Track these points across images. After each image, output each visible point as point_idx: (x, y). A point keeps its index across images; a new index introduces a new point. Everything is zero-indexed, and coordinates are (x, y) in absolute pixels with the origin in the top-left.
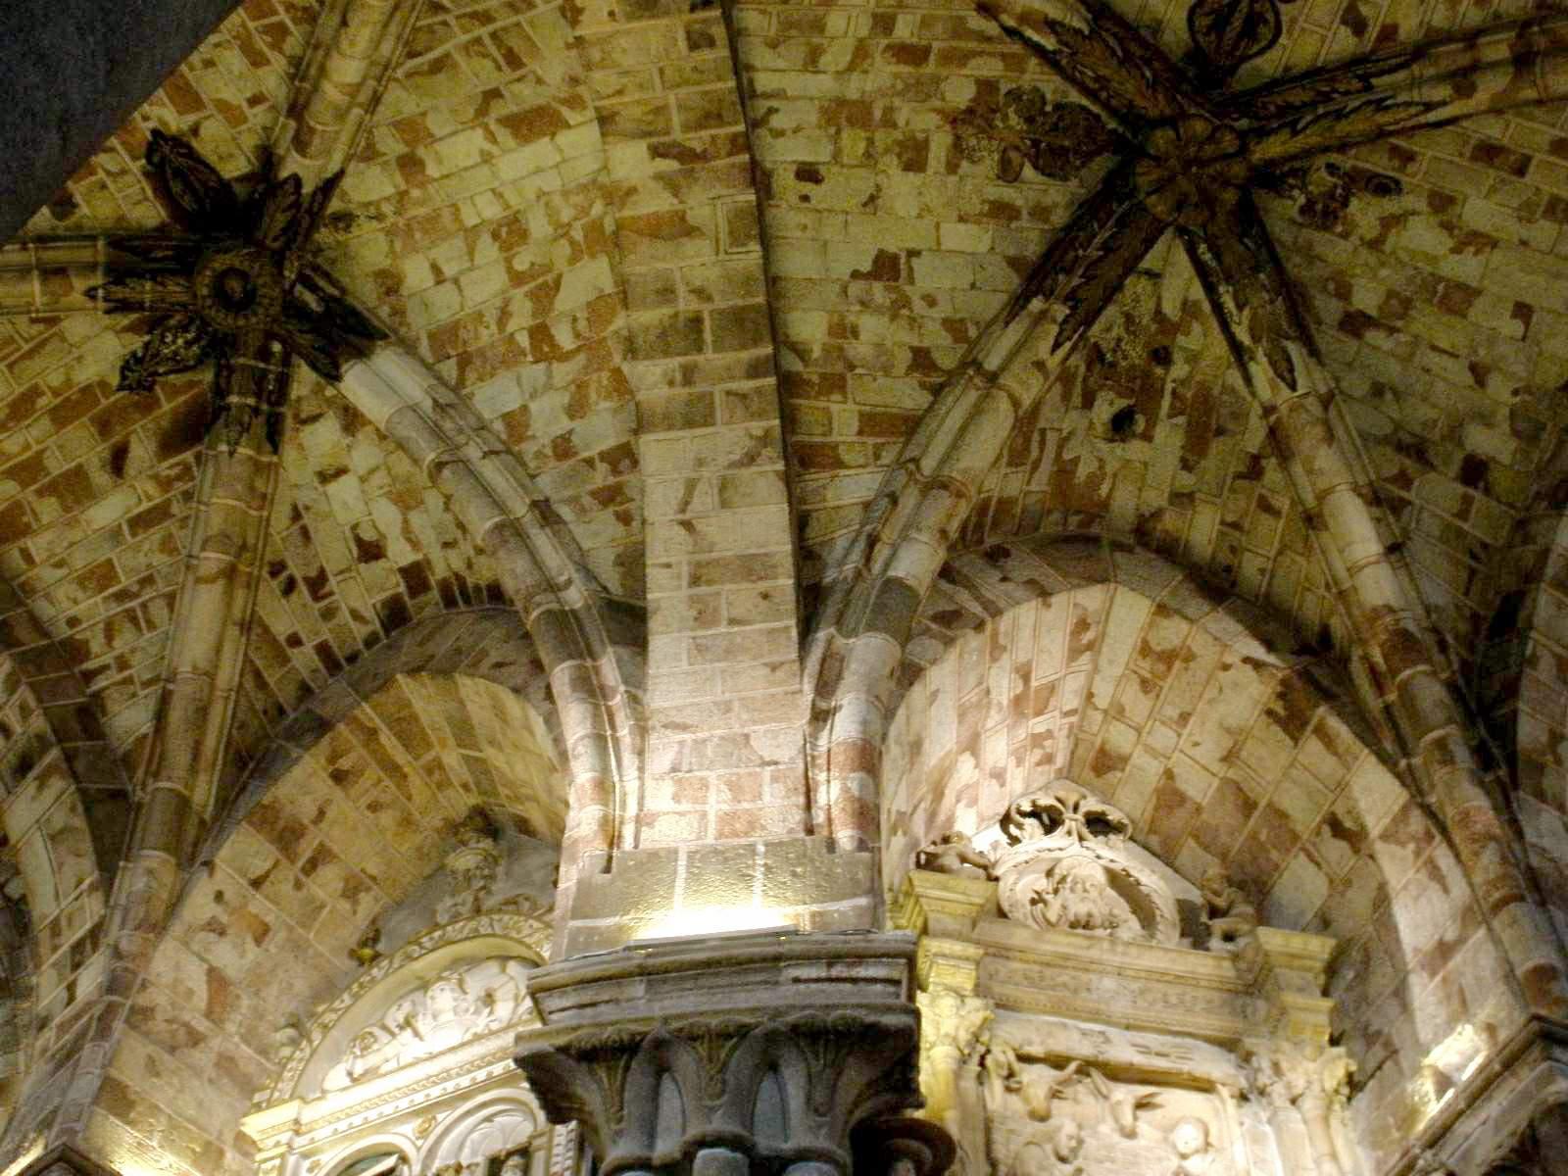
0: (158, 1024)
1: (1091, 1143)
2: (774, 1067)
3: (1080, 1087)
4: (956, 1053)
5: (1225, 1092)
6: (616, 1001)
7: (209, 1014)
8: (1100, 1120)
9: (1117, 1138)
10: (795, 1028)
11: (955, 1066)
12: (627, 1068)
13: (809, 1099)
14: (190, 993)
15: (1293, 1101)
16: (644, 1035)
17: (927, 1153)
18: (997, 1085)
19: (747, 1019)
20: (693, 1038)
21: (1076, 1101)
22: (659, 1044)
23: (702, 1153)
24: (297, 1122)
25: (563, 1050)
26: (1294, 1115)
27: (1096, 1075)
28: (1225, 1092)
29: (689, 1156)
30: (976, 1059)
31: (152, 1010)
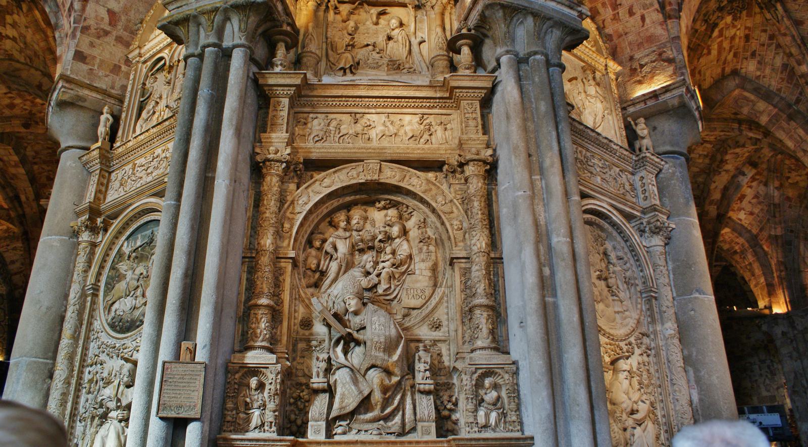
0: (93, 31)
1: (362, 28)
2: (229, 19)
3: (361, 10)
4: (316, 4)
5: (410, 7)
6: (187, 4)
7: (110, 24)
8: (367, 20)
9: (371, 25)
10: (231, 6)
11: (314, 8)
12: (188, 26)
13: (240, 28)
14: (103, 18)
15: (432, 7)
16: (190, 15)
17: (289, 40)
18: (331, 12)
19: (218, 5)
20: (204, 14)
21: (359, 14)
22: (195, 17)
23: (206, 49)
24: (139, 54)
25: (169, 23)
26: (433, 12)
27: (366, 6)
28: (410, 7)
29: (203, 51)
30: (324, 4)
31: (89, 26)
